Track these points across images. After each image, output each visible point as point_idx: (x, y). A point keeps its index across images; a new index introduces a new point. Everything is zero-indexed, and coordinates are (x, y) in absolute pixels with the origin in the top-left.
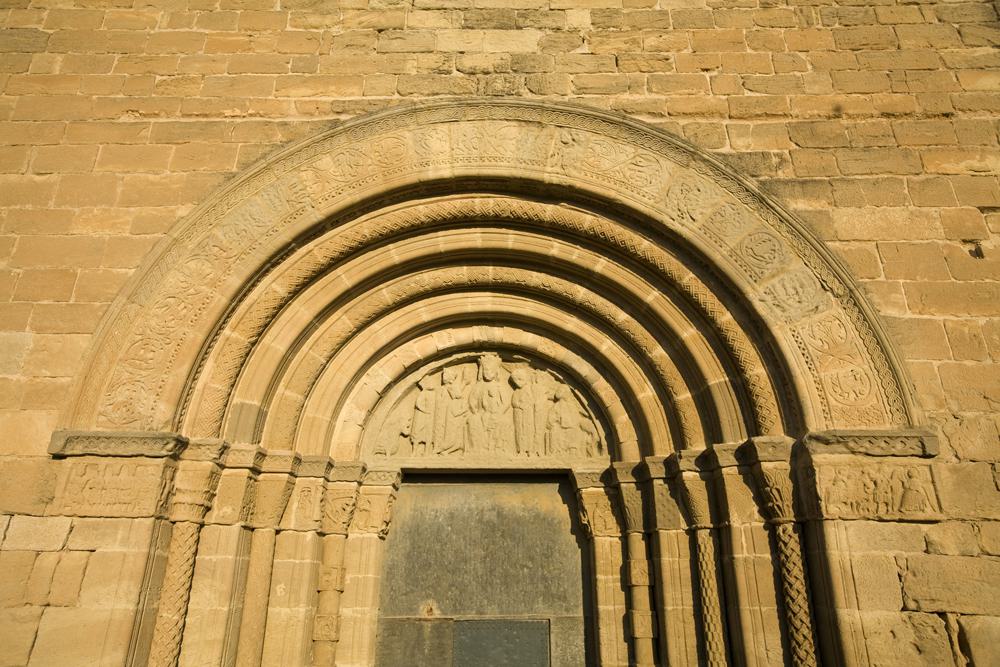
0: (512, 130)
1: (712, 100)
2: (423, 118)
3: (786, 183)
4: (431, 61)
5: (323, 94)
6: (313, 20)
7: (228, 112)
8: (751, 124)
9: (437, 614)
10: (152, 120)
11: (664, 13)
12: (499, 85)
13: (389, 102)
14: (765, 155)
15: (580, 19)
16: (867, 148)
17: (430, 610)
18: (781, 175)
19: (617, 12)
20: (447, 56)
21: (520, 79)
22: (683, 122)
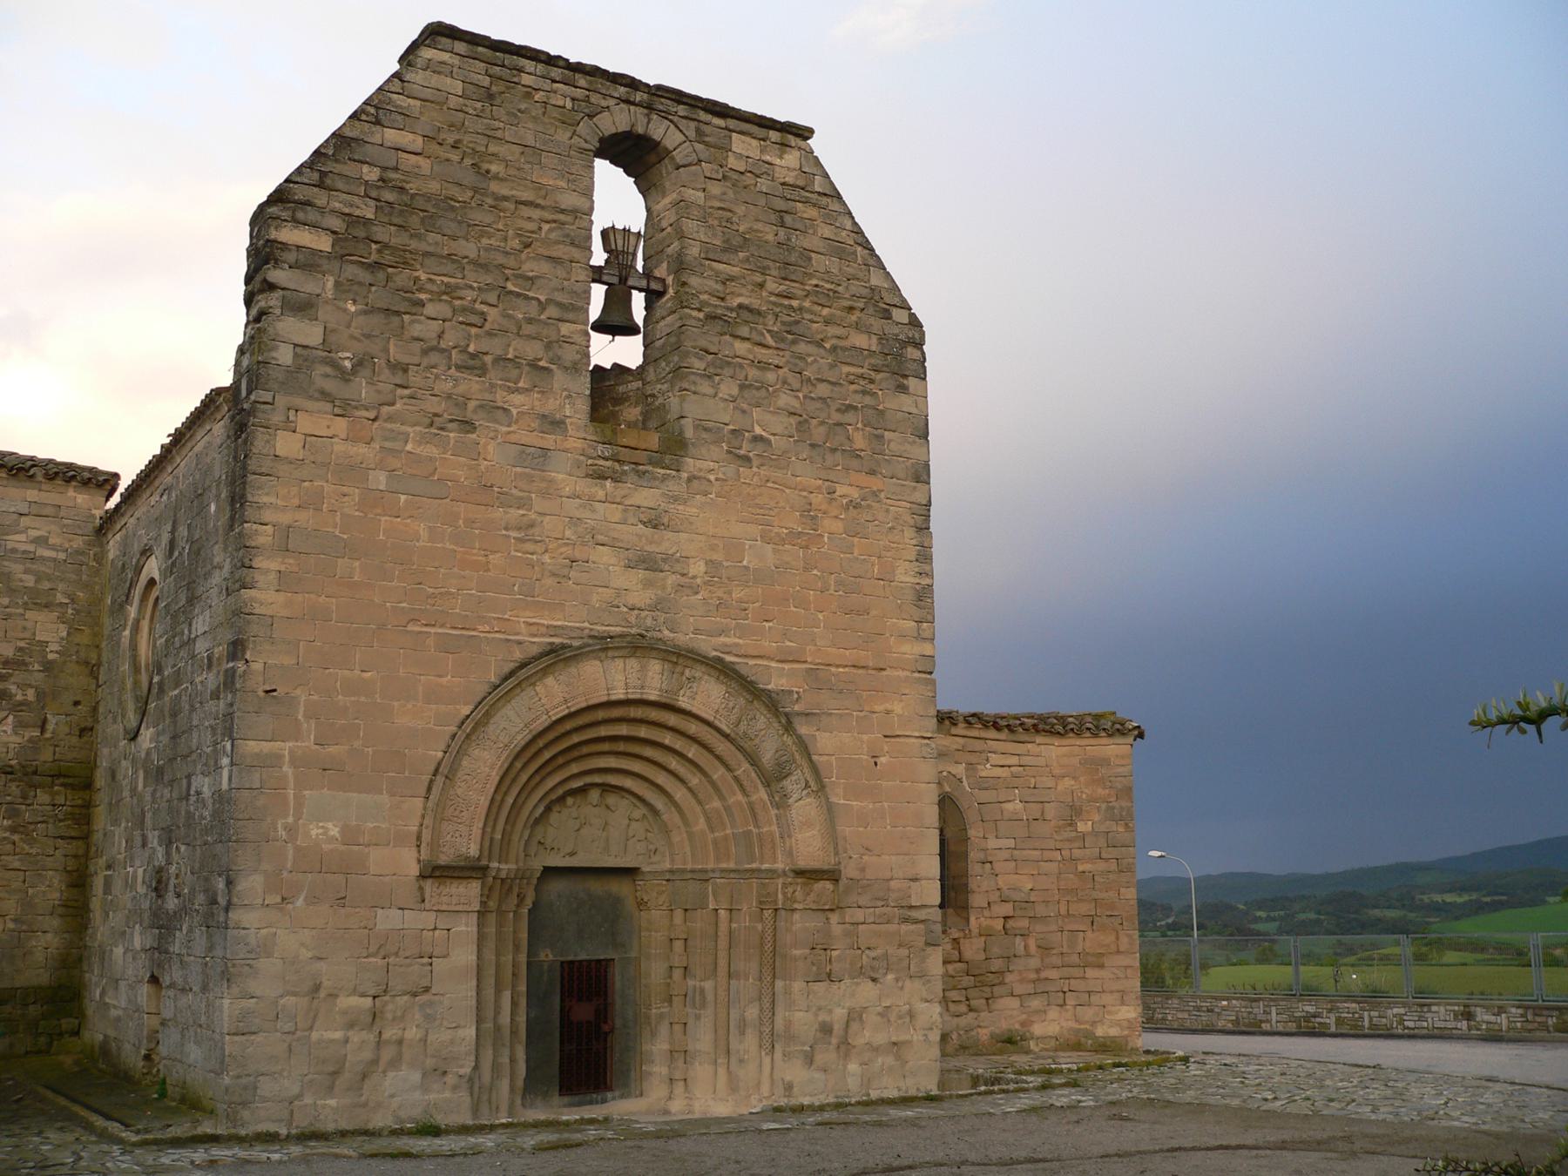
0: (655, 666)
1: (769, 645)
2: (610, 654)
3: (799, 714)
4: (607, 593)
5: (542, 617)
6: (530, 547)
7: (481, 628)
8: (786, 666)
9: (551, 957)
10: (432, 630)
11: (746, 568)
12: (649, 622)
13: (582, 629)
14: (791, 692)
15: (698, 568)
16: (841, 692)
17: (547, 956)
18: (796, 708)
19: (720, 563)
20: (619, 592)
21: (662, 617)
22: (752, 662)
